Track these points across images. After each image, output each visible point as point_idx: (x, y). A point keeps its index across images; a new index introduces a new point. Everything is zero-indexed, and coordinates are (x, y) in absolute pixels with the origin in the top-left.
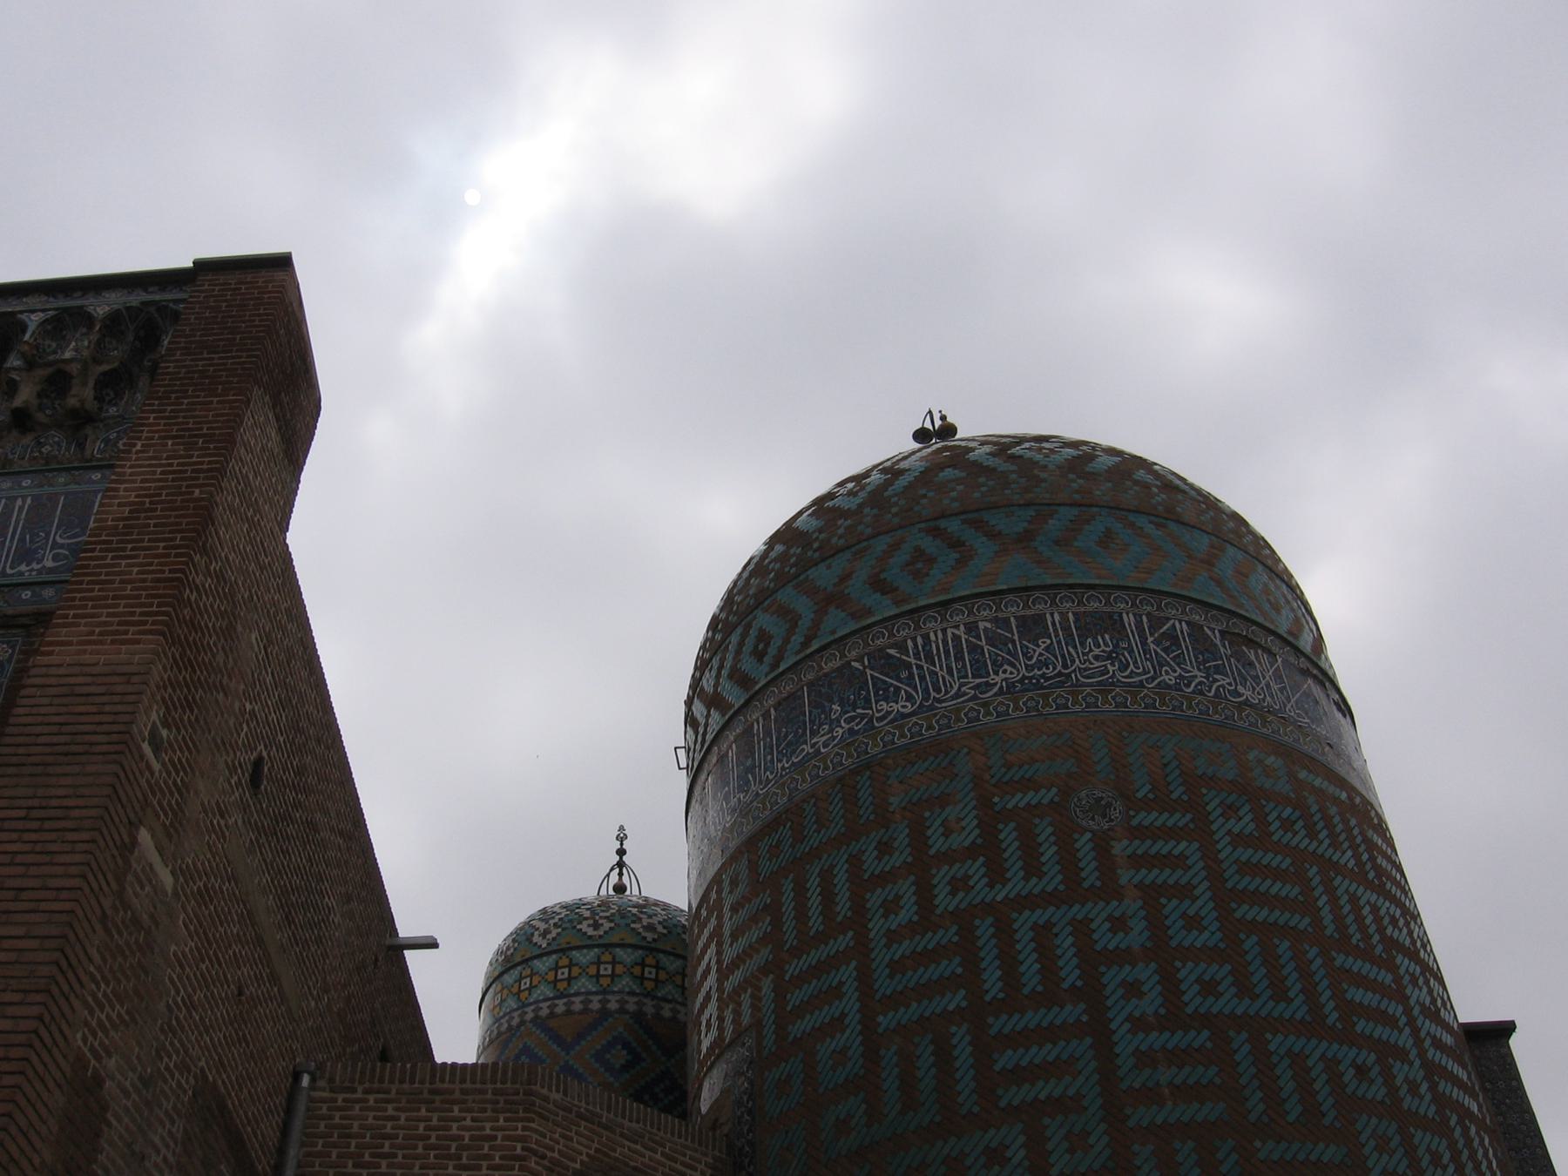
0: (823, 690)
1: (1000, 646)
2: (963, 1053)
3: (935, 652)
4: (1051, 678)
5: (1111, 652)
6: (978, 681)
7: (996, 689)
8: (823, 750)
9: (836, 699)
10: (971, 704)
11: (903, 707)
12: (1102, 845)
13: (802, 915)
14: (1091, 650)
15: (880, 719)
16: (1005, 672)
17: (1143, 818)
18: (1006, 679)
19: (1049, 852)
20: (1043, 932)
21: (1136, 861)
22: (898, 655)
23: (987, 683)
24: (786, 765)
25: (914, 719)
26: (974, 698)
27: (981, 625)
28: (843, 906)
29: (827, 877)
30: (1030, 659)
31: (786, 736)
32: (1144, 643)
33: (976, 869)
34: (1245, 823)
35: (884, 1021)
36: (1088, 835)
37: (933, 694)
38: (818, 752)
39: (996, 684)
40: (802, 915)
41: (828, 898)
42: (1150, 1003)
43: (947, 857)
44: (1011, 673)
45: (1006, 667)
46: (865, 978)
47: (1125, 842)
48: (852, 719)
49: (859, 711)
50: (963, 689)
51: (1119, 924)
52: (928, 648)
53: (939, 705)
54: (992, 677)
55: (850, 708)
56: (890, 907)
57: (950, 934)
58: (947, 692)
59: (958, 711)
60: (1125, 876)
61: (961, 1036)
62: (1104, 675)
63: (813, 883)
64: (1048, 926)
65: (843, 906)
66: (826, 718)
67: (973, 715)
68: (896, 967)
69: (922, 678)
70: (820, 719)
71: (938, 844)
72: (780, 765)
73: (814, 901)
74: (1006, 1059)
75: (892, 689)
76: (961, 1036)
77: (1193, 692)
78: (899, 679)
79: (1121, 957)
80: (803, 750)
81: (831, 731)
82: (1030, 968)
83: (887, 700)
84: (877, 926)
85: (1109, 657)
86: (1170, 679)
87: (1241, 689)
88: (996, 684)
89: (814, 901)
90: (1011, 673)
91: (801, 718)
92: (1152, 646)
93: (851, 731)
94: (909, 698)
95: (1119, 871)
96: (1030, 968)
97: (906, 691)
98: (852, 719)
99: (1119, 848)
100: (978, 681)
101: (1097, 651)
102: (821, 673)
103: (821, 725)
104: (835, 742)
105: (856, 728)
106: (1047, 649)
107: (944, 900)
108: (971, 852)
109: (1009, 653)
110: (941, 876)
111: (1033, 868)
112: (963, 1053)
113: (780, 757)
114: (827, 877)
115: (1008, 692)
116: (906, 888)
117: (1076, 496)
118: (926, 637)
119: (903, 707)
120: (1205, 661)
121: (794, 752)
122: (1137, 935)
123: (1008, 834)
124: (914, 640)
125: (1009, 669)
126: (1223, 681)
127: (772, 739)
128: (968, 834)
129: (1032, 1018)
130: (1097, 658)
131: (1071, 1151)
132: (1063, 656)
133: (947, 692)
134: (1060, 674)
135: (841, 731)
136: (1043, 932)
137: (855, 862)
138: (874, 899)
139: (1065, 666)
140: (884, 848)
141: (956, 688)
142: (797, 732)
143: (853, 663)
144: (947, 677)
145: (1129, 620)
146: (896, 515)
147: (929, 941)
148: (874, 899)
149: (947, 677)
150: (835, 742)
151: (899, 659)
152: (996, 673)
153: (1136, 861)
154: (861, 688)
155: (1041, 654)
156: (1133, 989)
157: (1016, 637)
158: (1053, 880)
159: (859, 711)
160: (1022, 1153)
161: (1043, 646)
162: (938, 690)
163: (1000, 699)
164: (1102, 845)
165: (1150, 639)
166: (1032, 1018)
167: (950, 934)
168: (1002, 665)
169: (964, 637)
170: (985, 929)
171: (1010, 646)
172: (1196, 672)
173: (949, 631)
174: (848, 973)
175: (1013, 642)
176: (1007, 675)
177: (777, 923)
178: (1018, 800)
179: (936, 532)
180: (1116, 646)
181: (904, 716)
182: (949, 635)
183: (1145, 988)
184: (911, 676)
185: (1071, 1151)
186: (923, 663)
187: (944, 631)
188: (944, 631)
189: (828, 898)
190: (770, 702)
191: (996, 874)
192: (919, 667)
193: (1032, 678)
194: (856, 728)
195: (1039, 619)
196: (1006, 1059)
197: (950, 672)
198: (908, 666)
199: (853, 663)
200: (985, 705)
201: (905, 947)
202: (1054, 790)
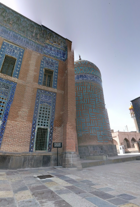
2: (89, 100)
12: (96, 91)
13: (78, 89)
17: (98, 90)
19: (93, 91)
20: (93, 95)
28: (82, 90)
29: (80, 88)
33: (90, 90)
35: (84, 97)
40: (78, 89)
41: (80, 89)
42: (97, 100)
46: (83, 94)
56: (85, 91)
57: (88, 93)
61: (88, 99)
65: (82, 90)
68: (85, 94)
71: (88, 88)
73: (80, 89)
74: (91, 101)
76: (88, 99)
79: (96, 97)
82: (92, 96)
84: (84, 91)
89: (80, 89)
96: (92, 96)
107: (88, 91)
108: (90, 89)
110: (88, 90)
112: (89, 100)
114: (80, 88)
116: (86, 90)
122: (97, 97)
123: (91, 89)
128: (89, 88)
129: (92, 99)
136: (93, 95)
137: (83, 87)
138: (84, 90)
140: (84, 87)
148: (84, 90)
156: (97, 99)
158: (93, 92)
164: (96, 91)
166: (92, 99)
167: (88, 93)
170: (90, 94)
174: (82, 94)
177: (77, 89)
189: (80, 89)
191: (91, 91)
196: (91, 101)
201: (85, 93)
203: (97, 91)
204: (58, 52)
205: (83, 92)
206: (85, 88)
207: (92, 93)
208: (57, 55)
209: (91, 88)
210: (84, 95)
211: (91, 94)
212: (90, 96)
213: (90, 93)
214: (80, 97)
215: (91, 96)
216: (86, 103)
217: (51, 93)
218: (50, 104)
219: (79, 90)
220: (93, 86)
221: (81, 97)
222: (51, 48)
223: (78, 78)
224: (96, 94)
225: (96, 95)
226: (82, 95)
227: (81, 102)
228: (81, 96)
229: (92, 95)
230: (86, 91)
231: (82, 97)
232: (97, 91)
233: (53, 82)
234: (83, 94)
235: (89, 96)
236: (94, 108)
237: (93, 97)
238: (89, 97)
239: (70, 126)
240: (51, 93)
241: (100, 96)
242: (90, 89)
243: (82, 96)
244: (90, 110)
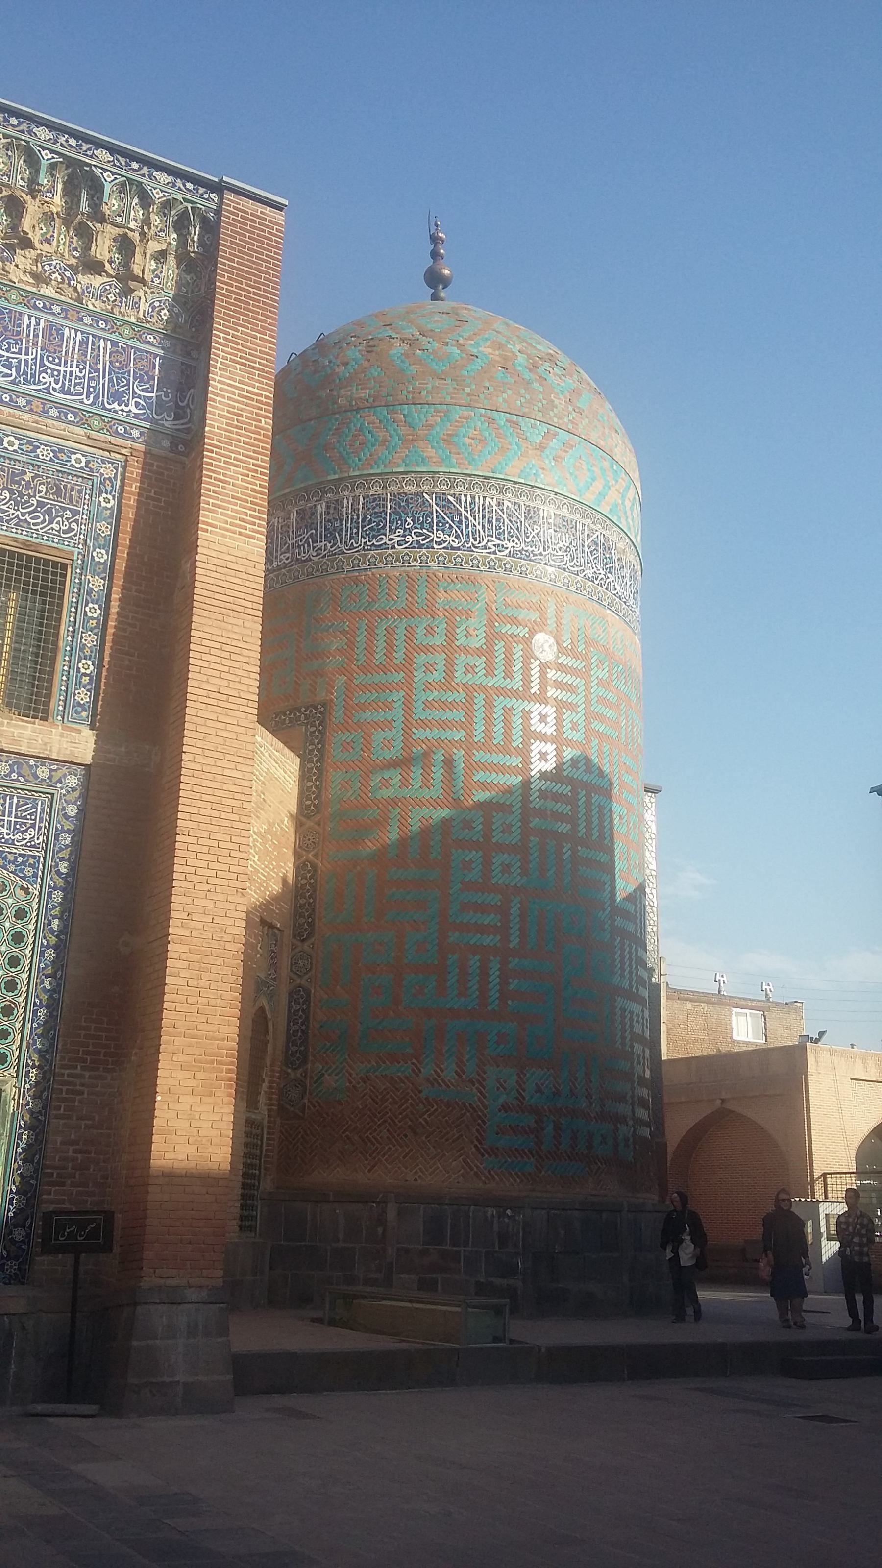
0: (402, 504)
1: (514, 522)
3: (477, 511)
4: (535, 555)
5: (568, 547)
6: (498, 542)
7: (507, 551)
8: (397, 546)
9: (410, 515)
10: (493, 556)
11: (453, 541)
14: (558, 543)
15: (439, 543)
16: (513, 541)
18: (514, 547)
21: (559, 685)
22: (455, 503)
23: (503, 546)
24: (368, 543)
25: (459, 552)
26: (495, 553)
27: (506, 503)
30: (528, 537)
31: (370, 523)
32: (583, 546)
33: (480, 662)
34: (603, 674)
36: (538, 662)
37: (472, 540)
38: (393, 547)
39: (507, 548)
43: (466, 650)
44: (517, 544)
45: (514, 538)
47: (554, 672)
48: (421, 534)
49: (425, 531)
50: (489, 544)
51: (543, 718)
52: (473, 506)
53: (474, 549)
54: (506, 542)
55: (419, 526)
56: (429, 668)
58: (480, 543)
59: (485, 557)
60: (551, 692)
62: (561, 562)
63: (381, 631)
64: (512, 709)
66: (401, 525)
67: (492, 563)
69: (467, 527)
70: (397, 524)
71: (461, 641)
72: (363, 540)
73: (381, 645)
75: (447, 525)
77: (598, 584)
78: (453, 521)
80: (383, 539)
81: (404, 536)
83: (443, 531)
84: (419, 675)
85: (566, 551)
86: (590, 572)
87: (616, 586)
88: (507, 548)
90: (517, 544)
91: (383, 515)
92: (586, 549)
93: (417, 542)
94: (457, 537)
95: (549, 688)
96: (499, 729)
97: (456, 532)
98: (421, 534)
99: (551, 674)
100: (498, 542)
101: (561, 545)
102: (402, 491)
103: (397, 528)
104: (407, 545)
105: (422, 542)
106: (537, 534)
107: (459, 675)
108: (479, 652)
109: (518, 529)
110: (461, 660)
111: (508, 675)
113: (364, 534)
114: (390, 632)
115: (513, 556)
116: (440, 659)
117: (570, 426)
118: (473, 498)
119: (453, 541)
120: (606, 564)
121: (374, 537)
123: (499, 646)
124: (466, 496)
125: (516, 541)
126: (612, 578)
127: (358, 515)
130: (560, 549)
131: (502, 832)
132: (544, 542)
133: (480, 543)
134: (541, 554)
135: (411, 540)
137: (410, 632)
138: (421, 659)
139: (544, 550)
141: (485, 541)
142: (378, 525)
143: (425, 495)
144: (482, 532)
145: (579, 527)
146: (469, 395)
147: (450, 697)
149: (482, 532)
150: (407, 545)
151: (454, 506)
152: (509, 540)
153: (559, 685)
154: (427, 516)
155: (534, 537)
157: (523, 520)
159: (425, 531)
160: (481, 827)
161: (536, 531)
162: (475, 540)
163: (508, 559)
165: (586, 544)
166: (497, 758)
168: (512, 536)
169: (495, 508)
170: (480, 700)
171: (519, 524)
172: (601, 571)
173: (487, 500)
175: (521, 522)
176: (514, 544)
178: (506, 629)
179: (491, 421)
180: (571, 544)
181: (453, 548)
182: (487, 503)
183: (549, 757)
184: (460, 522)
185: (502, 832)
186: (469, 515)
187: (484, 498)
188: (484, 498)
189: (390, 647)
190: (360, 490)
191: (490, 670)
192: (466, 518)
193: (526, 551)
194: (422, 542)
195: (536, 510)
197: (483, 527)
198: (461, 515)
199: (425, 495)
200: (500, 560)
202: (527, 629)
203: (561, 667)
204: (118, 370)
205: (410, 676)
206: (439, 640)
207: (502, 692)
208: (117, 397)
209: (492, 637)
210: (420, 713)
211: (489, 705)
212: (479, 729)
213: (483, 688)
214: (379, 736)
215: (489, 721)
216: (426, 794)
217: (43, 772)
218: (29, 871)
219: (379, 657)
220: (514, 621)
221: (389, 734)
222: (53, 332)
223: (377, 532)
224: (542, 699)
225: (536, 709)
226: (398, 714)
227: (386, 783)
228: (389, 724)
229: (498, 713)
230: (437, 676)
231: (396, 734)
232: (561, 667)
233: (61, 666)
234: (408, 705)
235: (467, 725)
236: (501, 848)
237: (508, 734)
238: (469, 735)
239: (189, 1075)
240: (43, 772)
241: (579, 718)
242: (479, 652)
243: (398, 724)
244: (467, 865)
